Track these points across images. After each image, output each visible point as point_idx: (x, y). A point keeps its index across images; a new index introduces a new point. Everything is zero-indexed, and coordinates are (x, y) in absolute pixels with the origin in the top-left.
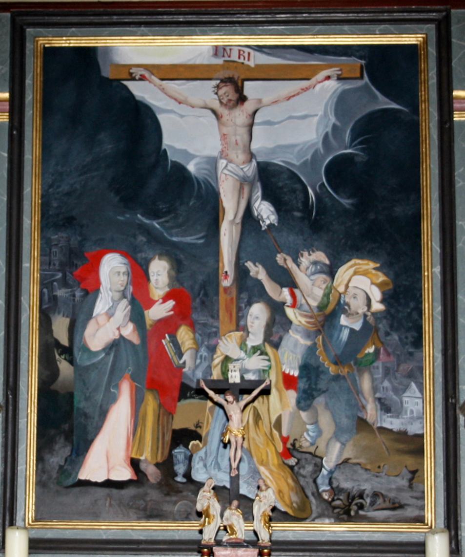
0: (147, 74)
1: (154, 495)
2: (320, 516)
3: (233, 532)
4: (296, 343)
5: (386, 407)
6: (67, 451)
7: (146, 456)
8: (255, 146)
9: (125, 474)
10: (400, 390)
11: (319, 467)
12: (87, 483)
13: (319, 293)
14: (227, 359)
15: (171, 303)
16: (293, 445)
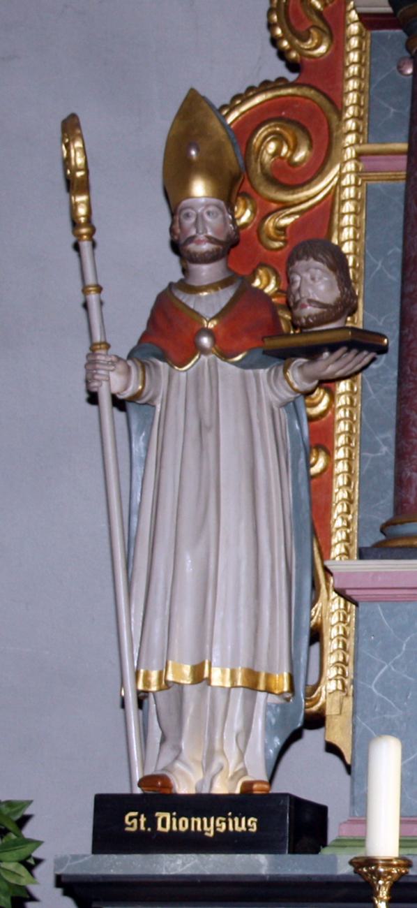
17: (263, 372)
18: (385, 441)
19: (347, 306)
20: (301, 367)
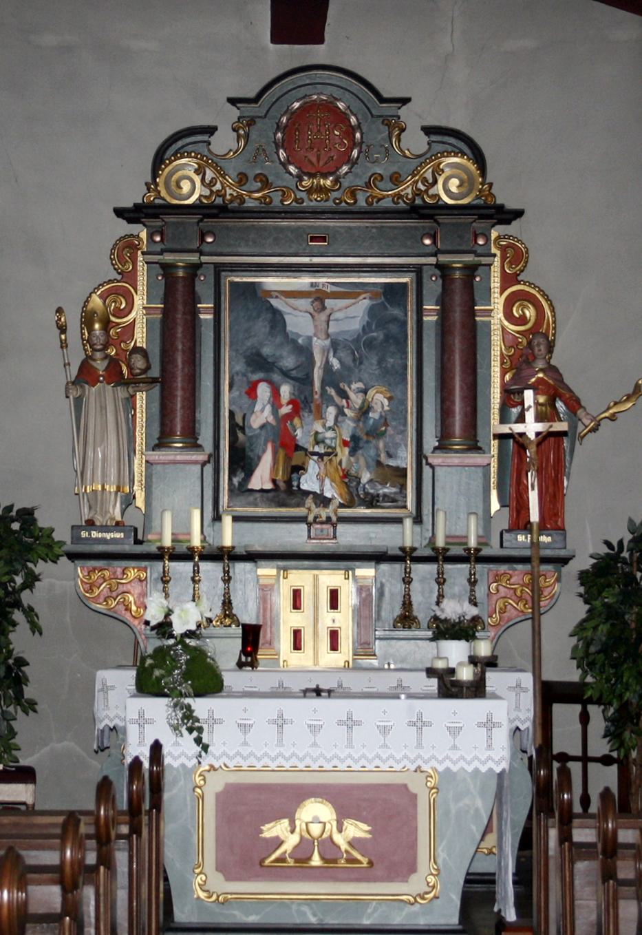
0: (279, 296)
1: (283, 496)
2: (360, 505)
3: (321, 517)
4: (349, 425)
5: (389, 456)
6: (242, 475)
7: (279, 477)
8: (330, 331)
9: (269, 486)
10: (397, 446)
11: (359, 483)
12: (252, 491)
13: (360, 402)
14: (317, 433)
15: (290, 406)
16: (347, 472)
17: (119, 388)
18: (155, 407)
19: (148, 368)
20: (133, 387)
